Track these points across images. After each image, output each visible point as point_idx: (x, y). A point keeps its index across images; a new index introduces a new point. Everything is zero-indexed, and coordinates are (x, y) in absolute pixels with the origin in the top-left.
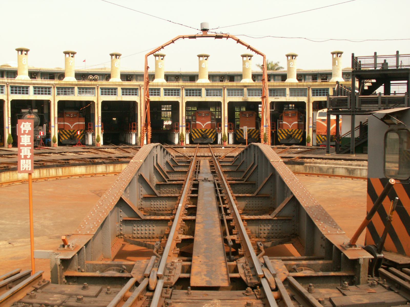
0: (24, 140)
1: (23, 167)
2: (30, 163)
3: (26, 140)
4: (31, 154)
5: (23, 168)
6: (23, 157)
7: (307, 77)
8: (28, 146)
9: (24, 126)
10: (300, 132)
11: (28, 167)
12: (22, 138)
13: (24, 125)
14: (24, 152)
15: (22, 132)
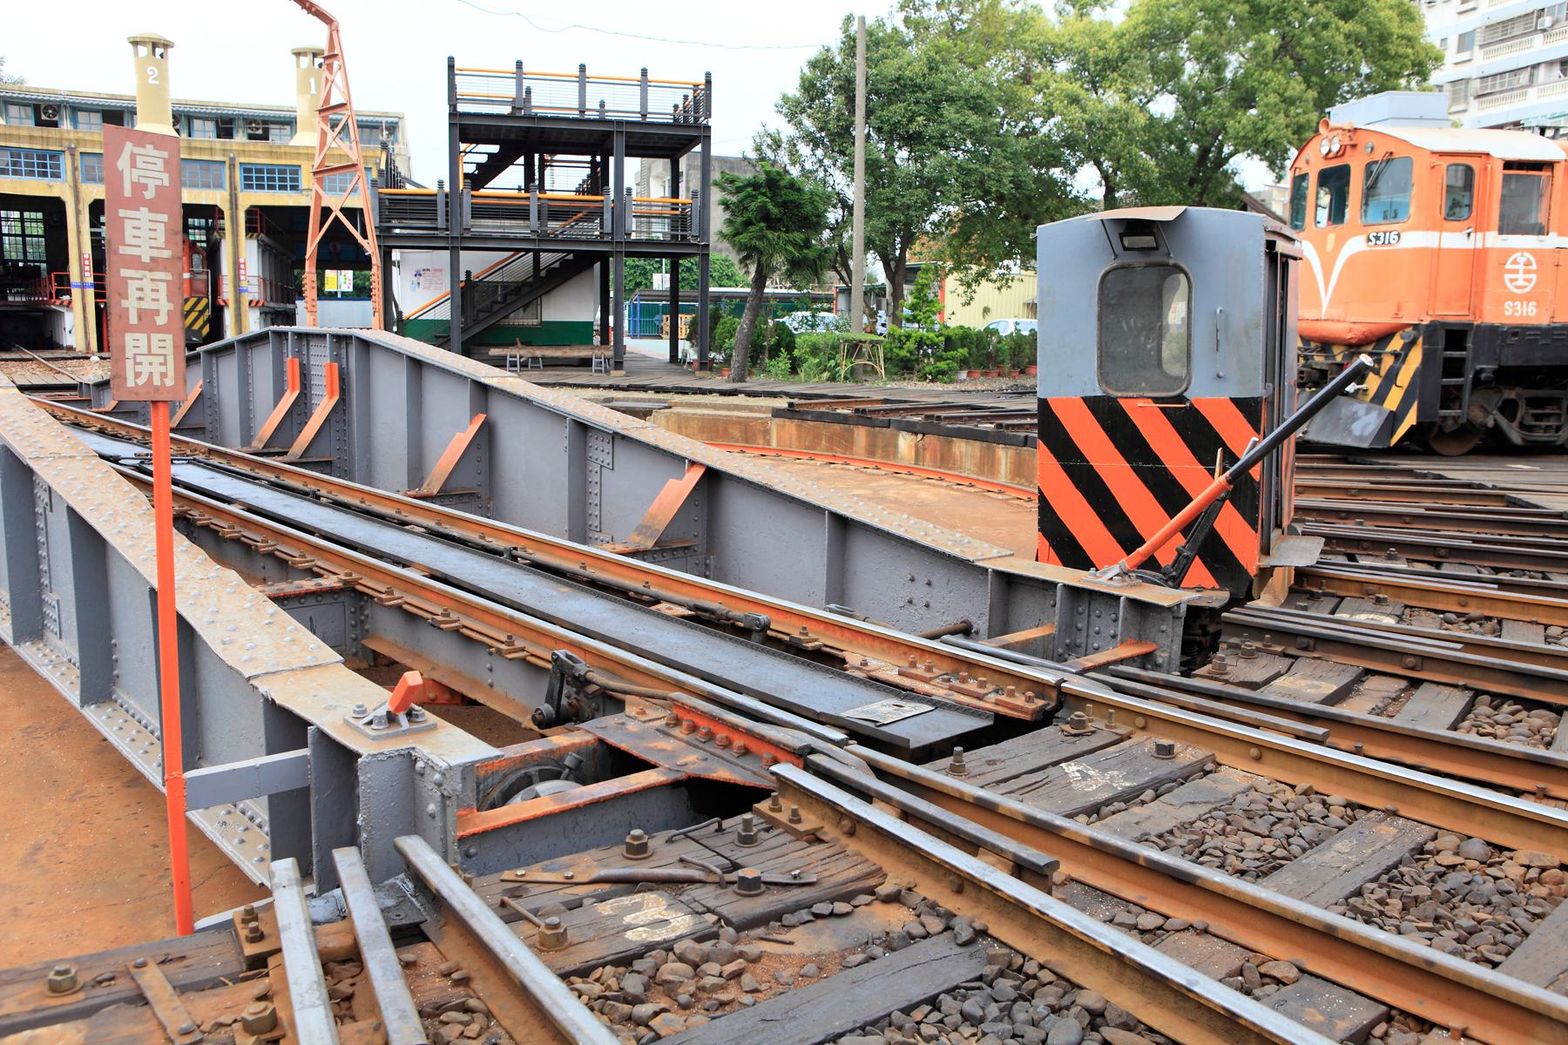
0: (136, 233)
1: (139, 368)
2: (169, 351)
3: (145, 233)
4: (170, 306)
5: (138, 375)
6: (133, 320)
7: (197, 124)
8: (155, 264)
9: (133, 165)
10: (200, 307)
11: (163, 369)
12: (128, 224)
13: (133, 156)
14: (139, 294)
15: (128, 193)
